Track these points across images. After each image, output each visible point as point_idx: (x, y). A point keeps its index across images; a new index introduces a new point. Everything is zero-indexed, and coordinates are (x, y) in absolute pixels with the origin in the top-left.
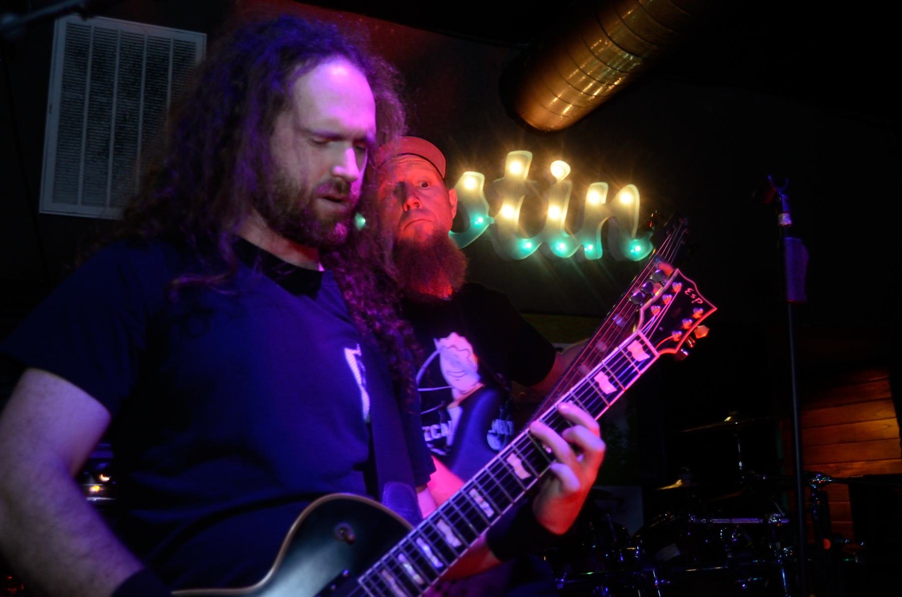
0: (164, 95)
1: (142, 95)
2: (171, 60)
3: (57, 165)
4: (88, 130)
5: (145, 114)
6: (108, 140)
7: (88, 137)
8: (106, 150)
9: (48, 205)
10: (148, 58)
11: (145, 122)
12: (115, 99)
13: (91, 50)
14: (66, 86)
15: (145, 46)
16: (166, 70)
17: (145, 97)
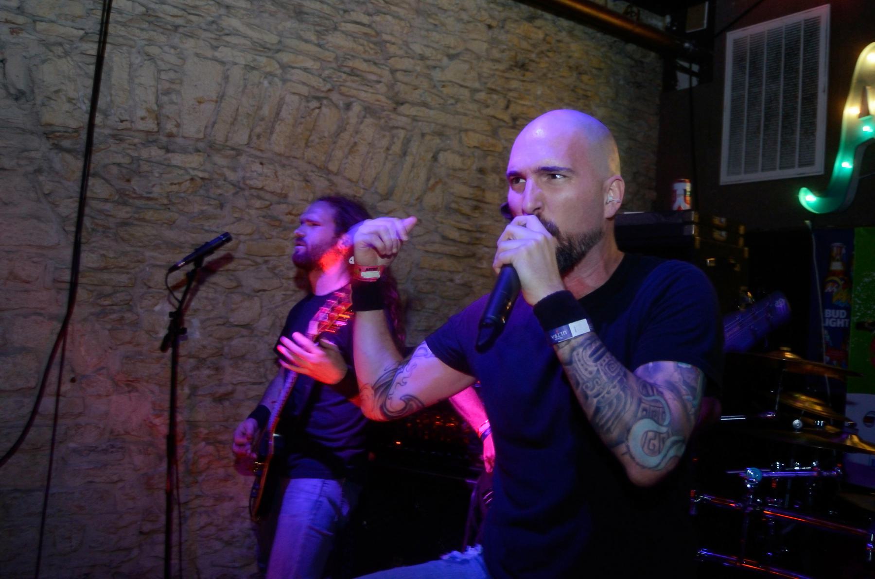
0: (797, 71)
1: (782, 76)
2: (802, 40)
3: (730, 148)
4: (748, 116)
5: (785, 91)
6: (760, 121)
7: (748, 120)
8: (758, 128)
9: (725, 179)
10: (786, 45)
11: (785, 97)
12: (764, 87)
13: (748, 54)
14: (734, 88)
15: (783, 36)
16: (799, 49)
17: (785, 78)
